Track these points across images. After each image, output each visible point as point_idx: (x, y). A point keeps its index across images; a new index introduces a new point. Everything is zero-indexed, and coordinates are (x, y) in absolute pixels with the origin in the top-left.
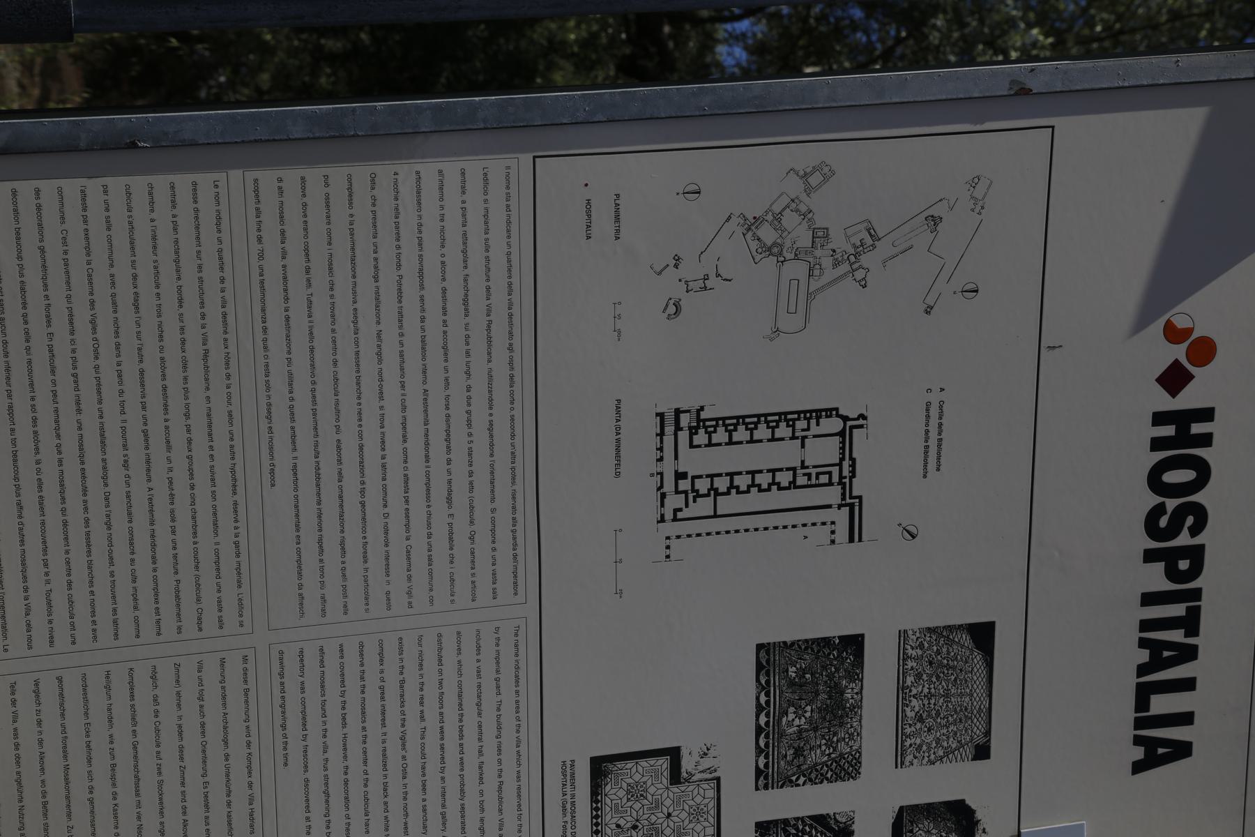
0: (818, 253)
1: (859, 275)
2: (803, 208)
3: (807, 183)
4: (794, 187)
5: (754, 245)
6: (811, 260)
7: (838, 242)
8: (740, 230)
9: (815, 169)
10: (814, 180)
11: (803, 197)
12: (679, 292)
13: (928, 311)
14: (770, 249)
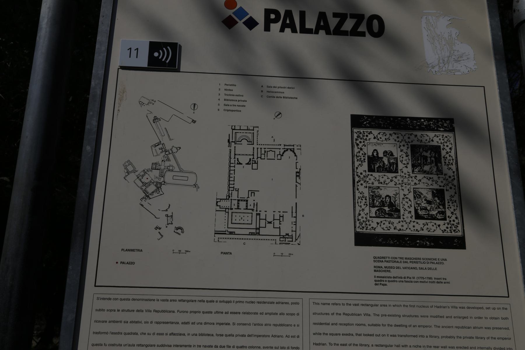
0: (162, 167)
1: (174, 150)
2: (142, 173)
3: (131, 172)
4: (132, 177)
5: (155, 194)
6: (165, 170)
7: (158, 159)
8: (148, 201)
9: (126, 168)
10: (130, 168)
11: (137, 173)
12: (172, 228)
13: (194, 121)
14: (158, 188)
